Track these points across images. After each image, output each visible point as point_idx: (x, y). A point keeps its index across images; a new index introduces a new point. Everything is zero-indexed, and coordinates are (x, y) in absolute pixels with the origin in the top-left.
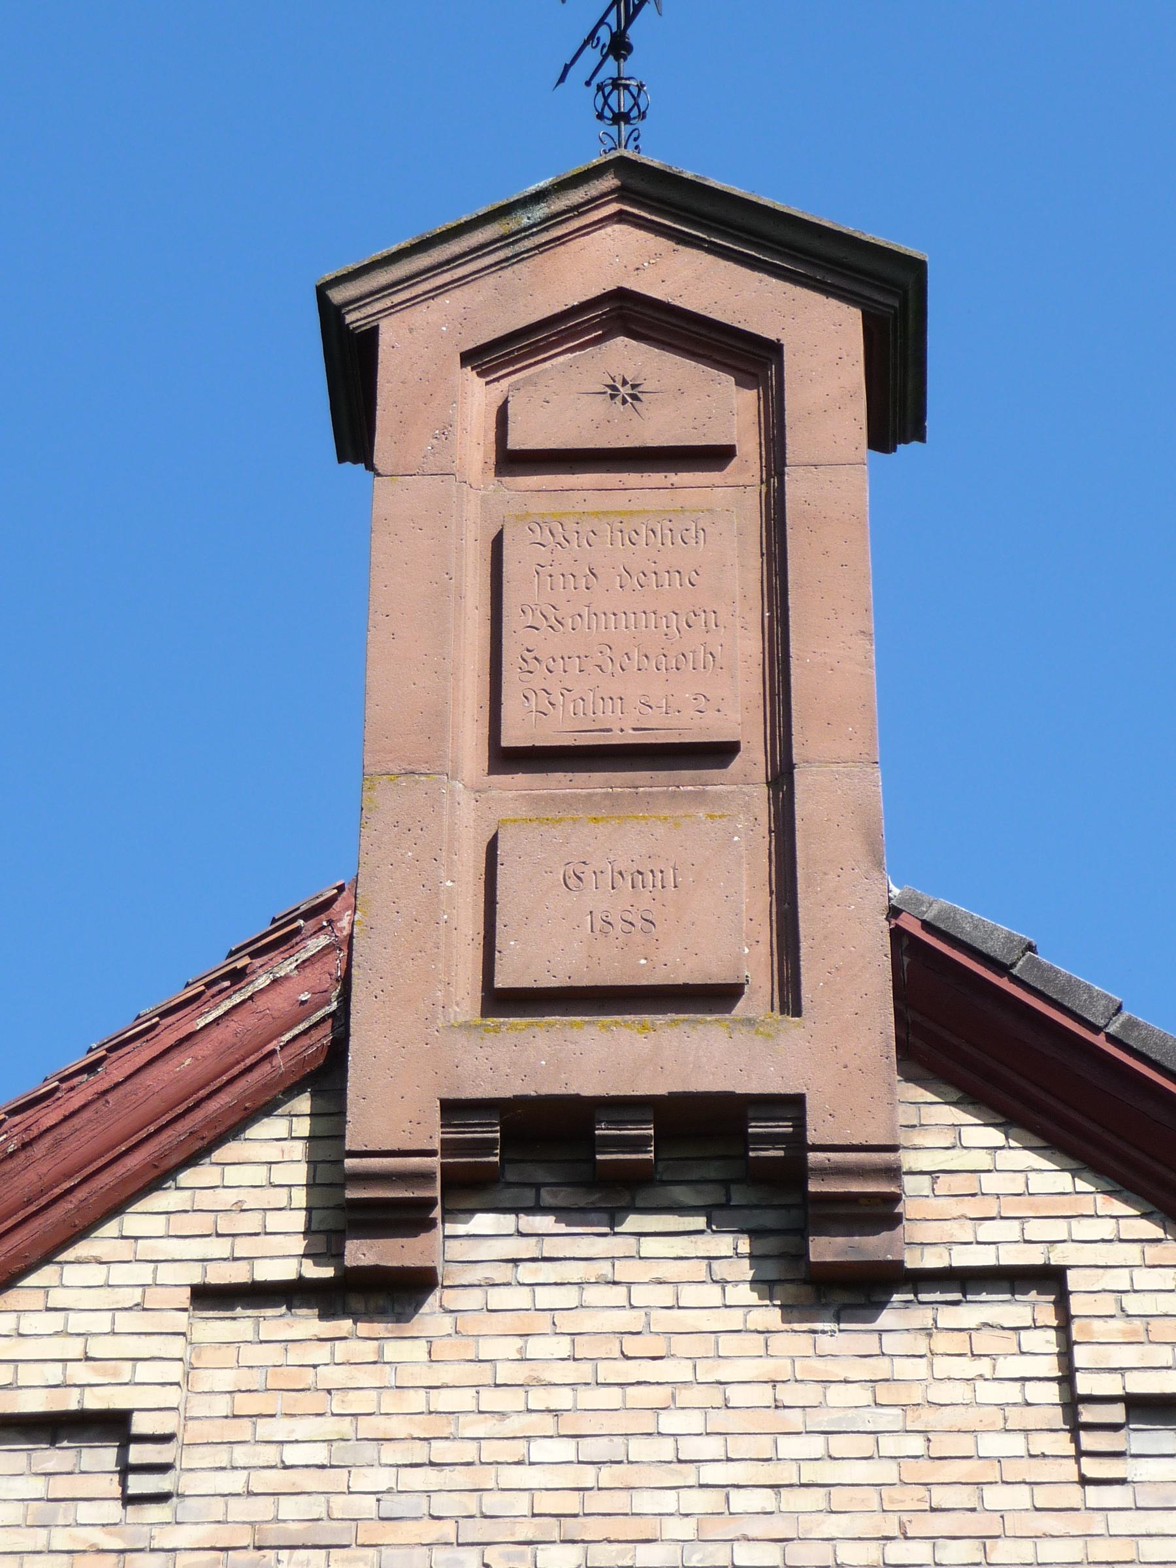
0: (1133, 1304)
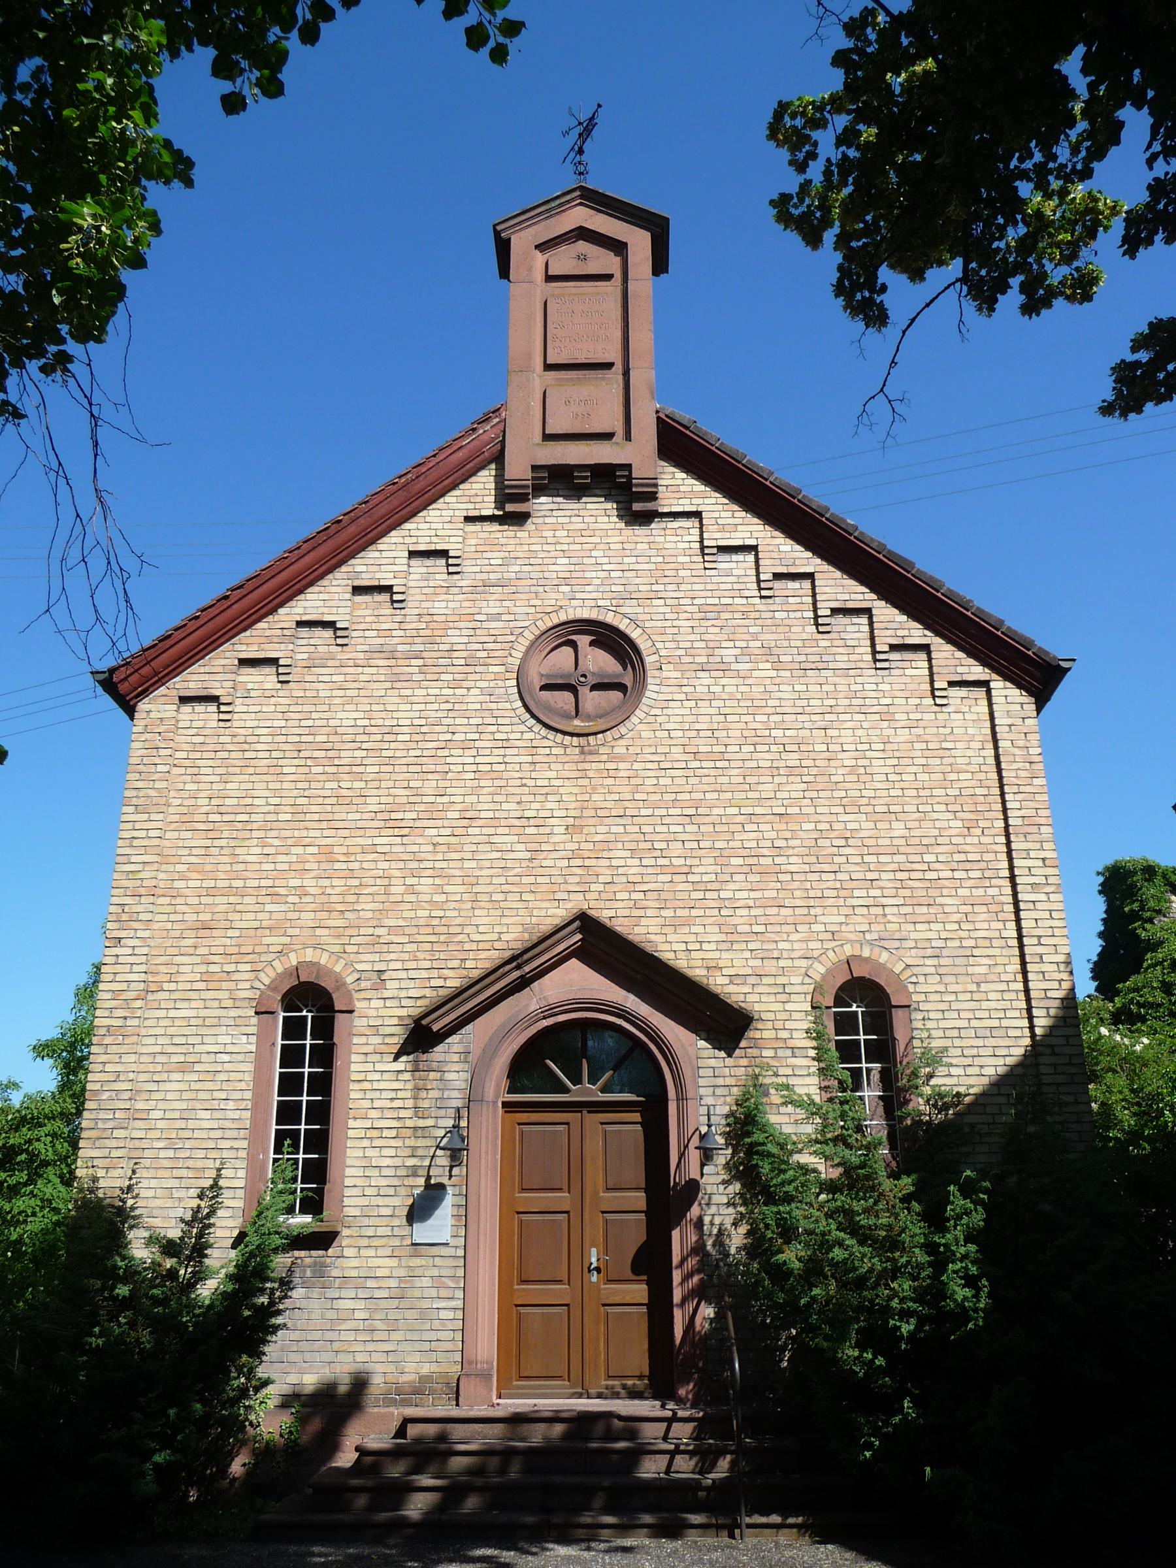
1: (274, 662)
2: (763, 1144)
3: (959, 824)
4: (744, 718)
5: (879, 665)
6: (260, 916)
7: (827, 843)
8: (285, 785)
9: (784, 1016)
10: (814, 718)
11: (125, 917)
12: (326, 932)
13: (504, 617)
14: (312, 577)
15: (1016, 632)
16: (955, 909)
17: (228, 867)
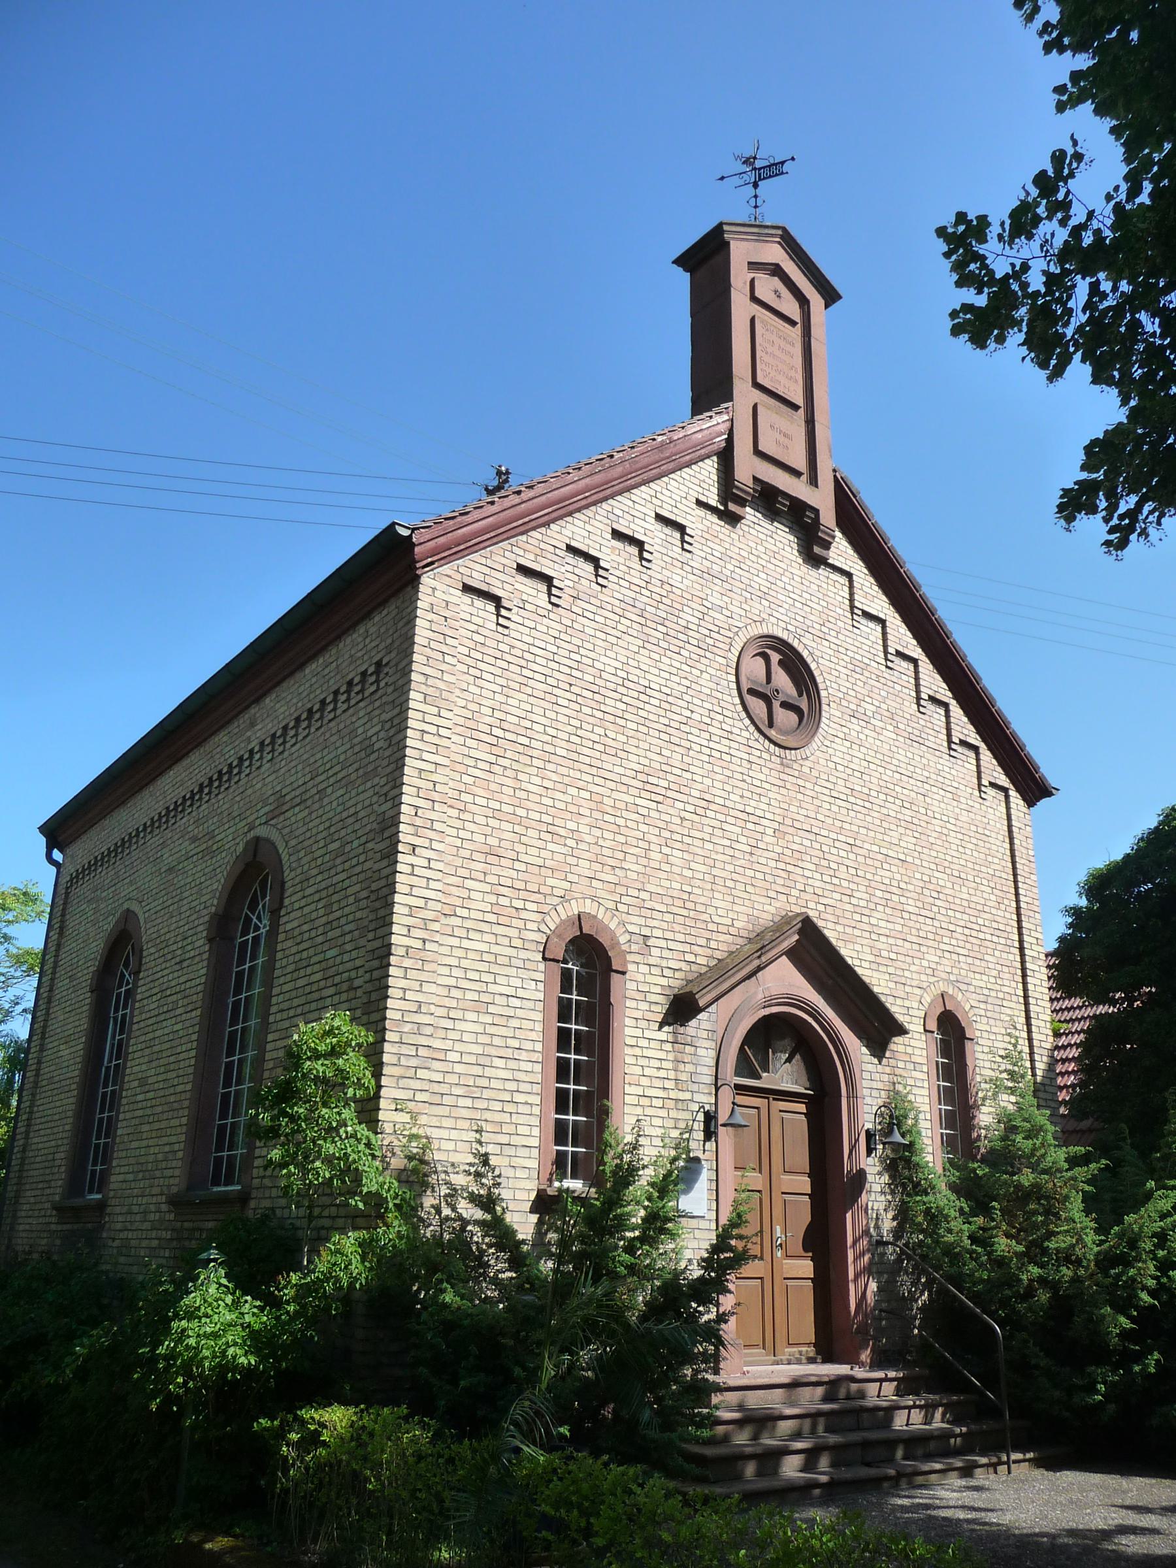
1: (548, 580)
6: (544, 854)
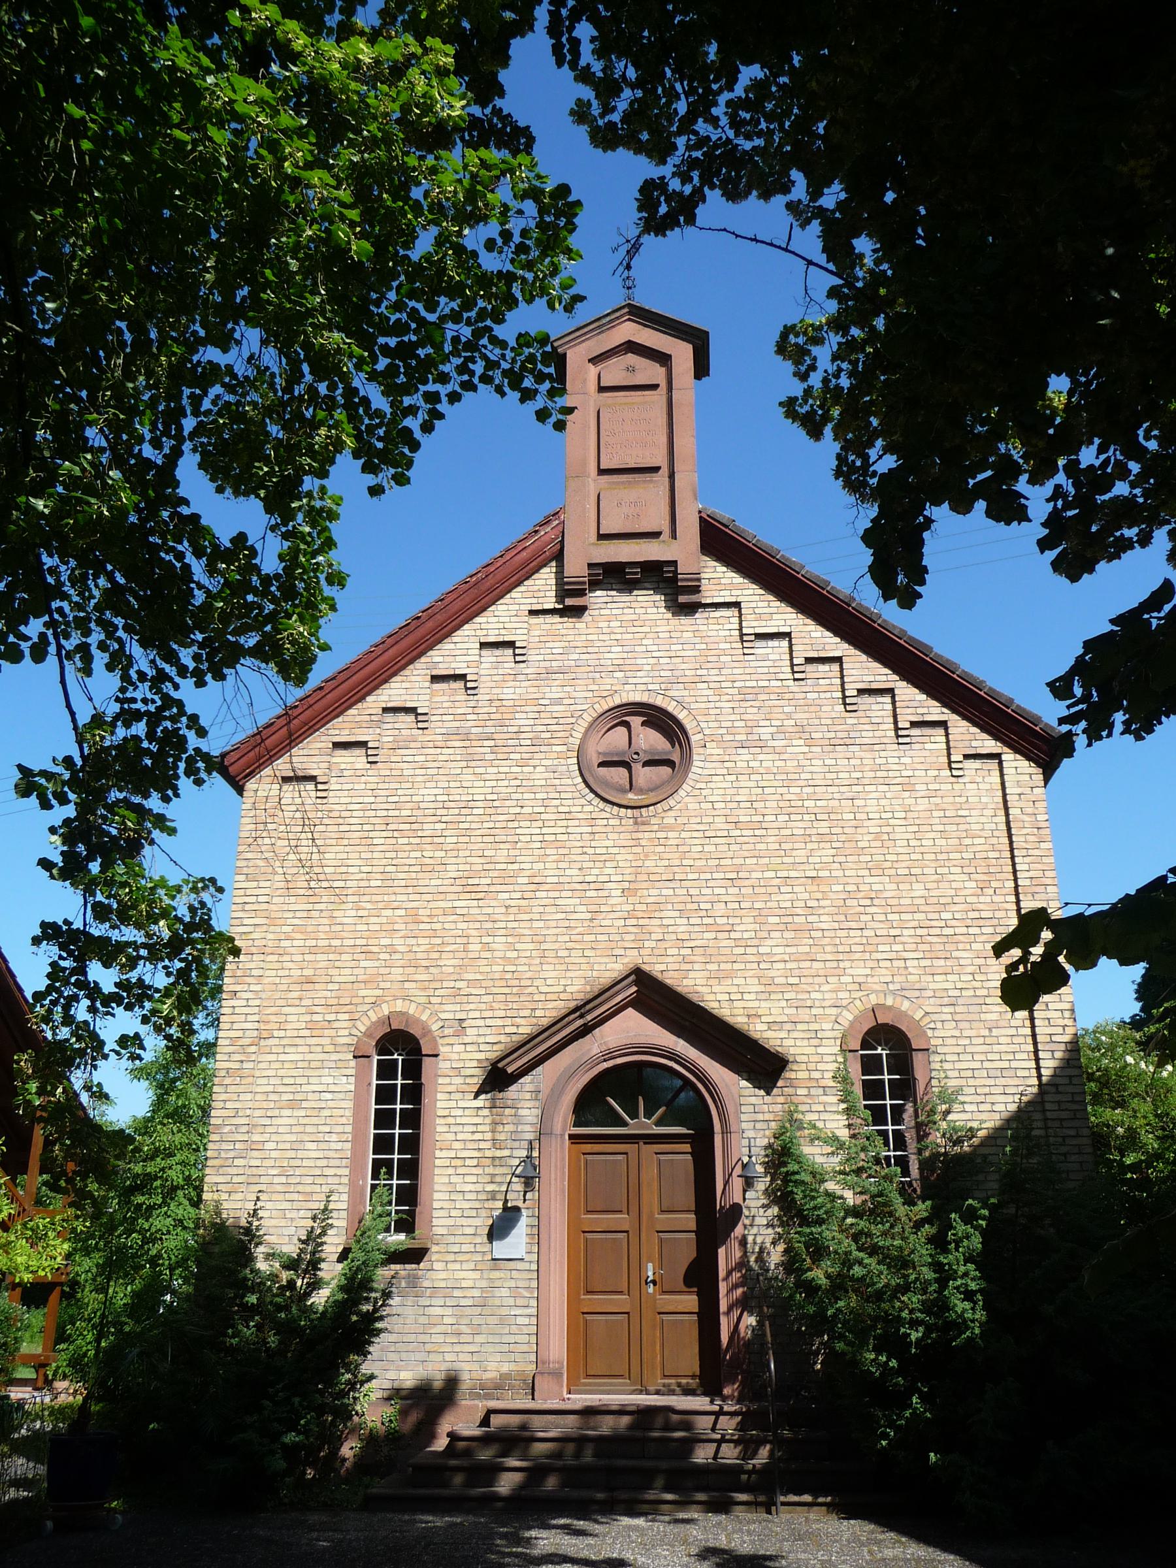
0: (757, 611)
2: (797, 1173)
3: (974, 884)
4: (780, 790)
5: (901, 740)
6: (356, 971)
7: (855, 903)
8: (376, 855)
9: (816, 1058)
10: (843, 789)
11: (239, 973)
12: (413, 985)
13: (566, 701)
14: (396, 667)
15: (1024, 709)
16: (969, 962)
17: (327, 928)
